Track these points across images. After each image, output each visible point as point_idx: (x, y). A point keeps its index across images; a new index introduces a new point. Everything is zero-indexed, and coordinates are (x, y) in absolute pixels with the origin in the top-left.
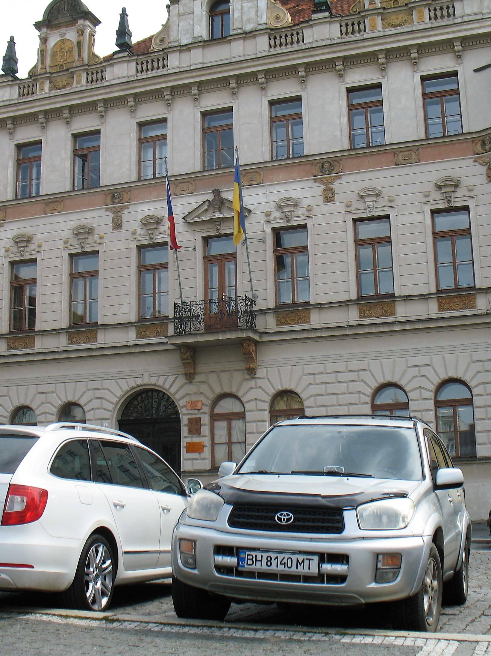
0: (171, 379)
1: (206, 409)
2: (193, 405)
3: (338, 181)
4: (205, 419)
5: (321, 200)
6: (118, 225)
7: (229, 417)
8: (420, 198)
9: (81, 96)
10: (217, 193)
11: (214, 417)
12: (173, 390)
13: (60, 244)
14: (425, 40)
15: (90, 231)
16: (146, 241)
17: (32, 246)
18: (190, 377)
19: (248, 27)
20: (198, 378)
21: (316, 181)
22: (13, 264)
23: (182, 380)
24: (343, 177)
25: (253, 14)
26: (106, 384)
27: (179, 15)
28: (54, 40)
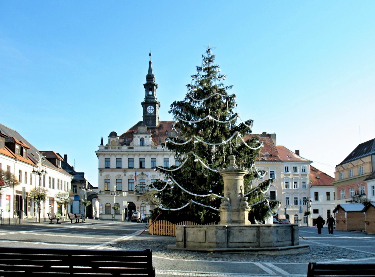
0: (134, 201)
1: (140, 206)
2: (138, 205)
4: (140, 207)
6: (125, 175)
7: (143, 207)
10: (142, 172)
11: (141, 207)
13: (114, 177)
15: (120, 175)
16: (130, 178)
17: (109, 177)
18: (138, 200)
19: (148, 145)
20: (139, 201)
22: (105, 179)
23: (136, 201)
25: (148, 142)
27: (135, 140)
28: (112, 139)
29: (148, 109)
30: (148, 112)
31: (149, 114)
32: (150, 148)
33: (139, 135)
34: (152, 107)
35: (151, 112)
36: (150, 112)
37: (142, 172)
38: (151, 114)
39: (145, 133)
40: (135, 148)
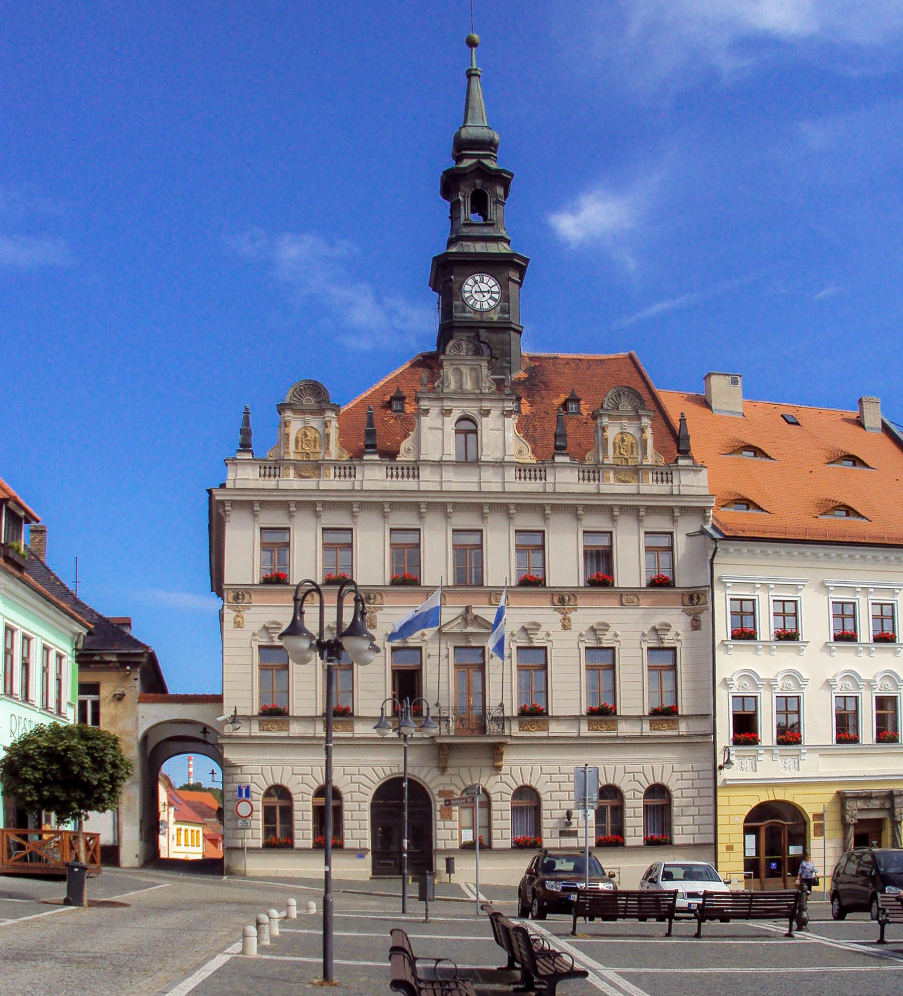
0: (425, 770)
3: (574, 613)
5: (559, 626)
8: (638, 636)
9: (339, 494)
12: (427, 780)
14: (653, 504)
18: (443, 769)
20: (450, 771)
21: (555, 609)
23: (436, 772)
24: (579, 610)
26: (363, 770)
29: (467, 288)
30: (471, 303)
31: (476, 311)
32: (511, 474)
33: (448, 404)
34: (486, 279)
35: (486, 306)
36: (478, 306)
37: (468, 609)
38: (482, 312)
39: (479, 398)
40: (425, 473)
